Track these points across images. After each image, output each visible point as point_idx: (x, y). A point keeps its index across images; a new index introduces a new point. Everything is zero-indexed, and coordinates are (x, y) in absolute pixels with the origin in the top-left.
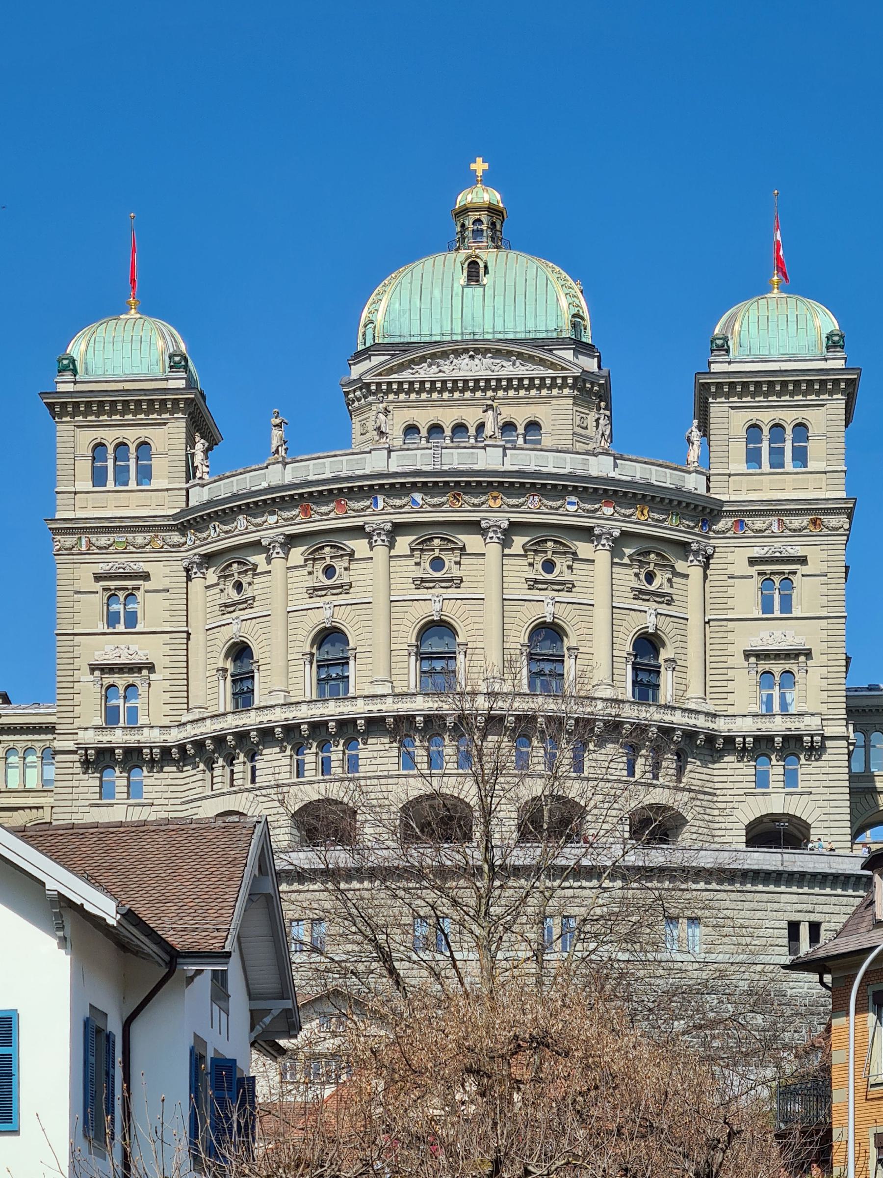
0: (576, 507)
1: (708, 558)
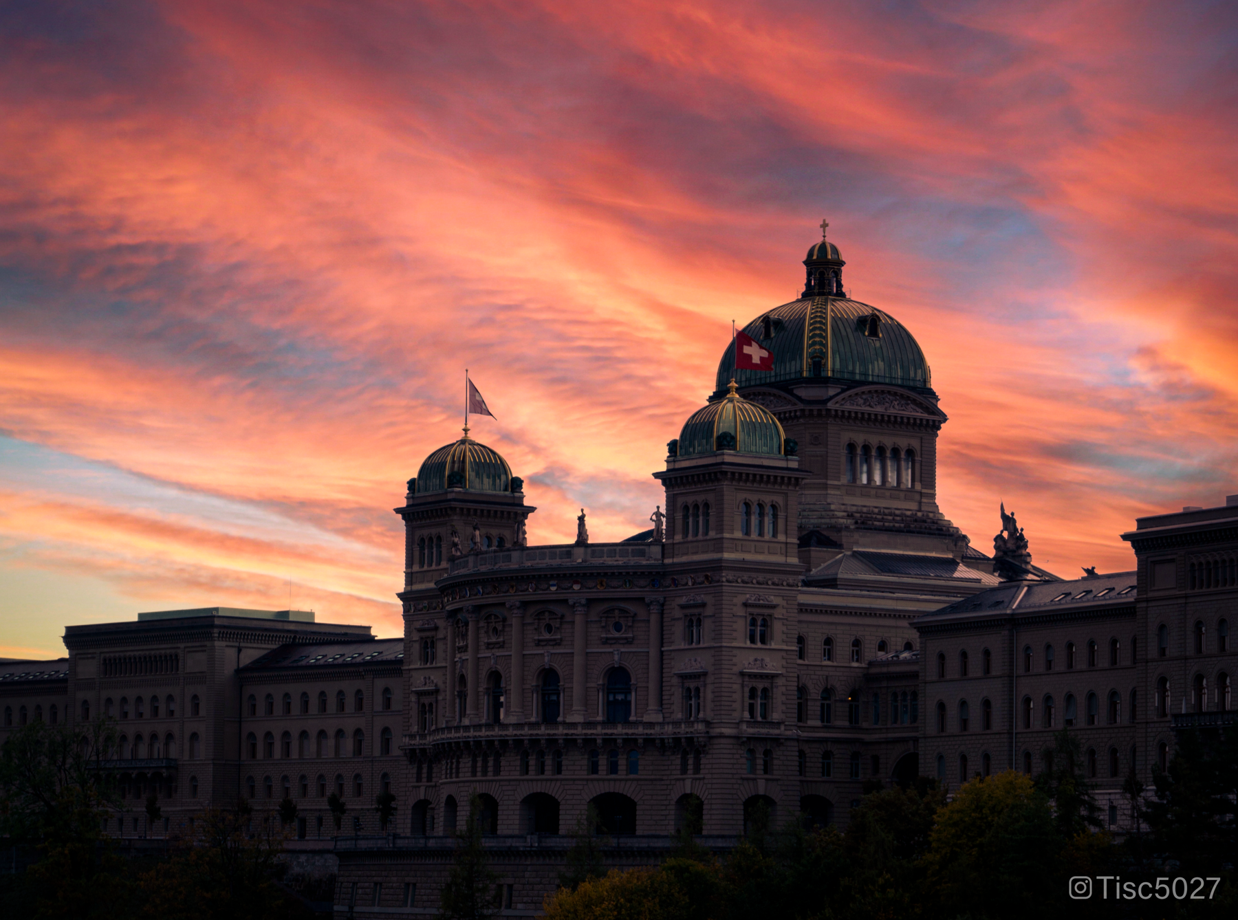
1: (663, 605)
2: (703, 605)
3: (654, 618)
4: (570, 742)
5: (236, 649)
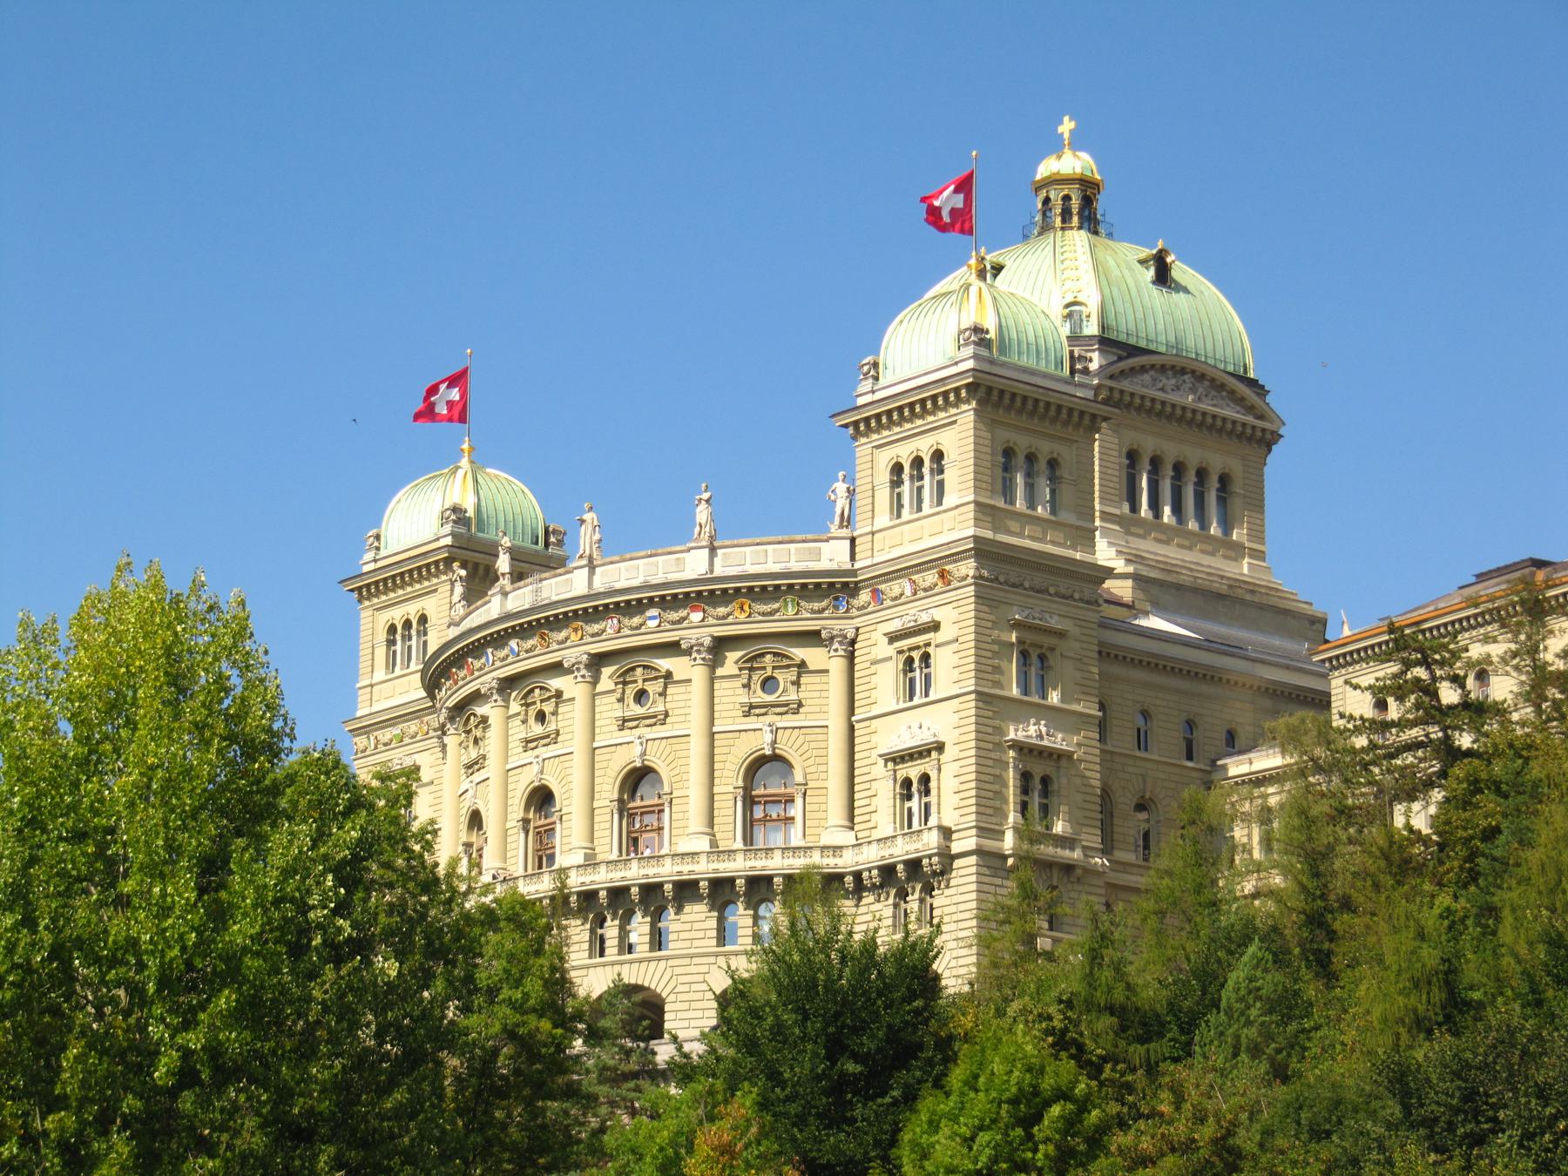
0: (656, 622)
1: (853, 642)
2: (935, 626)
3: (837, 666)
4: (686, 890)
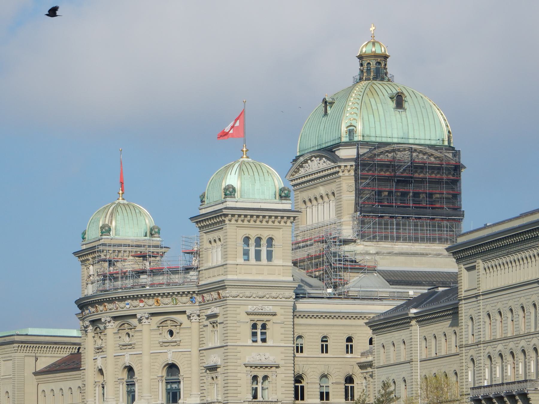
5: (34, 358)
